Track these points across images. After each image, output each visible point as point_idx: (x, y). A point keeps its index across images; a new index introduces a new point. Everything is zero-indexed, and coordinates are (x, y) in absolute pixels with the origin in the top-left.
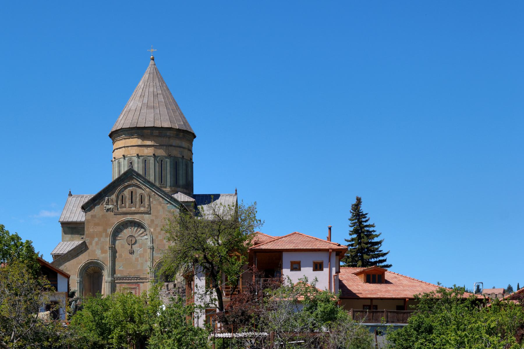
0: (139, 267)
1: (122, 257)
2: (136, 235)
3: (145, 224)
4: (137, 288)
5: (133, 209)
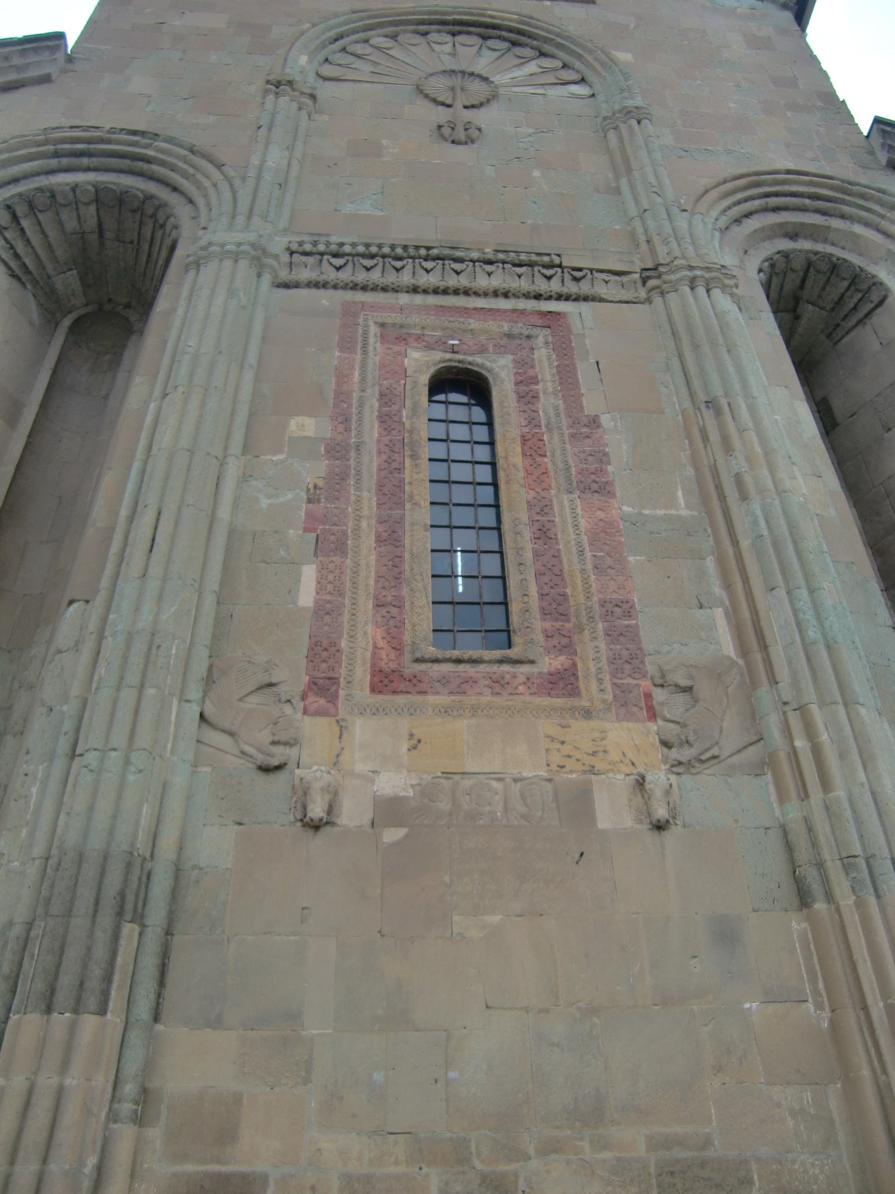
4: (529, 337)
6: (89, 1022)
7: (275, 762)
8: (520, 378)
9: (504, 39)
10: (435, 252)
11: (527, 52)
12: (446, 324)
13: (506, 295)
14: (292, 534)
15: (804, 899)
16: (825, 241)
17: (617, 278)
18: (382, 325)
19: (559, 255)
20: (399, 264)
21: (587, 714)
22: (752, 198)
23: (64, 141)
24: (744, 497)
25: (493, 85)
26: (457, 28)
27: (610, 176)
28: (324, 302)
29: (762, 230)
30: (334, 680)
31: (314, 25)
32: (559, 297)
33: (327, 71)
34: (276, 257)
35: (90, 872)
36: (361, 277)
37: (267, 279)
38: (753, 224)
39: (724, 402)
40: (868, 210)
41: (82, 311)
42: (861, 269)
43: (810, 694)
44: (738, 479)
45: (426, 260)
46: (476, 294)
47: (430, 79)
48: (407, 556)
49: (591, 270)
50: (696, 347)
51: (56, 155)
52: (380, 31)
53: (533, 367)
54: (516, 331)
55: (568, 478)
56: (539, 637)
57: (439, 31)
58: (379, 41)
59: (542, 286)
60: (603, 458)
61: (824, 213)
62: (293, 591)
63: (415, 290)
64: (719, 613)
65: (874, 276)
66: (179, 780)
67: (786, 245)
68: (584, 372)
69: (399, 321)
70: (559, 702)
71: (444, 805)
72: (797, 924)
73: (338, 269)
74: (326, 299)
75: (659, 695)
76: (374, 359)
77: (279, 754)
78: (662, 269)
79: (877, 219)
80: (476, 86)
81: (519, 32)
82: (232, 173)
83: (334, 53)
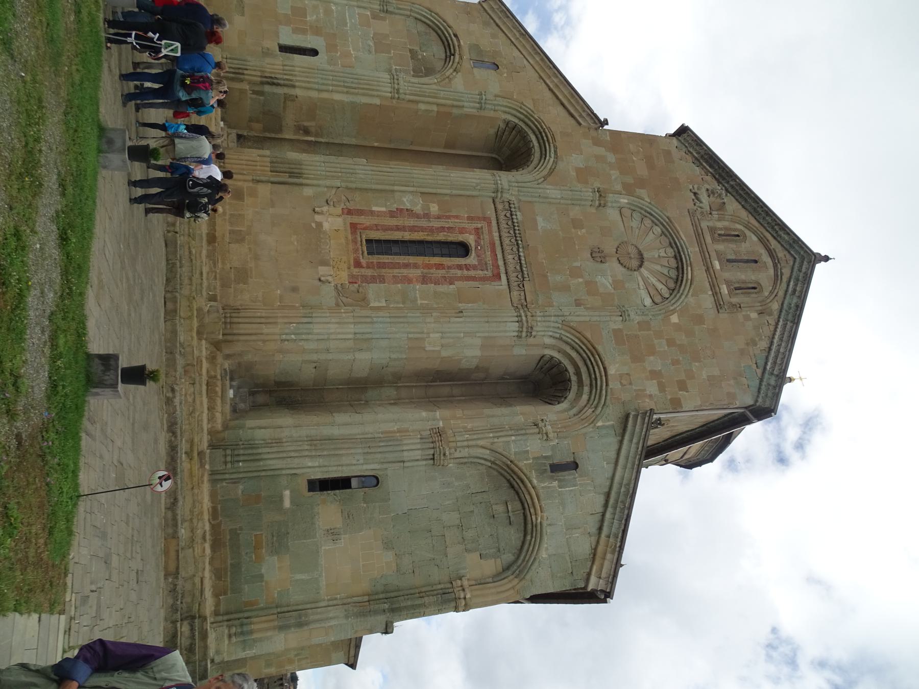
0: (555, 279)
1: (575, 227)
2: (642, 270)
3: (686, 296)
4: (487, 269)
8: (468, 266)
9: (678, 276)
10: (520, 242)
12: (486, 245)
13: (505, 264)
16: (579, 386)
17: (523, 298)
18: (482, 228)
20: (512, 232)
21: (349, 268)
22: (587, 354)
23: (546, 133)
26: (679, 258)
28: (489, 213)
29: (573, 359)
31: (650, 203)
33: (627, 212)
34: (502, 196)
35: (298, 166)
37: (493, 195)
38: (574, 354)
39: (460, 315)
40: (594, 400)
41: (500, 159)
42: (566, 398)
45: (516, 240)
46: (503, 255)
51: (540, 133)
53: (474, 270)
54: (488, 265)
55: (426, 274)
56: (371, 261)
58: (657, 230)
60: (437, 283)
61: (591, 385)
62: (377, 205)
63: (500, 237)
64: (385, 305)
65: (563, 402)
66: (321, 182)
67: (571, 370)
68: (476, 284)
69: (484, 232)
70: (352, 262)
71: (322, 236)
73: (505, 215)
74: (491, 213)
75: (356, 285)
76: (466, 226)
78: (525, 309)
79: (591, 402)
80: (635, 263)
81: (682, 281)
82: (540, 181)
83: (641, 213)
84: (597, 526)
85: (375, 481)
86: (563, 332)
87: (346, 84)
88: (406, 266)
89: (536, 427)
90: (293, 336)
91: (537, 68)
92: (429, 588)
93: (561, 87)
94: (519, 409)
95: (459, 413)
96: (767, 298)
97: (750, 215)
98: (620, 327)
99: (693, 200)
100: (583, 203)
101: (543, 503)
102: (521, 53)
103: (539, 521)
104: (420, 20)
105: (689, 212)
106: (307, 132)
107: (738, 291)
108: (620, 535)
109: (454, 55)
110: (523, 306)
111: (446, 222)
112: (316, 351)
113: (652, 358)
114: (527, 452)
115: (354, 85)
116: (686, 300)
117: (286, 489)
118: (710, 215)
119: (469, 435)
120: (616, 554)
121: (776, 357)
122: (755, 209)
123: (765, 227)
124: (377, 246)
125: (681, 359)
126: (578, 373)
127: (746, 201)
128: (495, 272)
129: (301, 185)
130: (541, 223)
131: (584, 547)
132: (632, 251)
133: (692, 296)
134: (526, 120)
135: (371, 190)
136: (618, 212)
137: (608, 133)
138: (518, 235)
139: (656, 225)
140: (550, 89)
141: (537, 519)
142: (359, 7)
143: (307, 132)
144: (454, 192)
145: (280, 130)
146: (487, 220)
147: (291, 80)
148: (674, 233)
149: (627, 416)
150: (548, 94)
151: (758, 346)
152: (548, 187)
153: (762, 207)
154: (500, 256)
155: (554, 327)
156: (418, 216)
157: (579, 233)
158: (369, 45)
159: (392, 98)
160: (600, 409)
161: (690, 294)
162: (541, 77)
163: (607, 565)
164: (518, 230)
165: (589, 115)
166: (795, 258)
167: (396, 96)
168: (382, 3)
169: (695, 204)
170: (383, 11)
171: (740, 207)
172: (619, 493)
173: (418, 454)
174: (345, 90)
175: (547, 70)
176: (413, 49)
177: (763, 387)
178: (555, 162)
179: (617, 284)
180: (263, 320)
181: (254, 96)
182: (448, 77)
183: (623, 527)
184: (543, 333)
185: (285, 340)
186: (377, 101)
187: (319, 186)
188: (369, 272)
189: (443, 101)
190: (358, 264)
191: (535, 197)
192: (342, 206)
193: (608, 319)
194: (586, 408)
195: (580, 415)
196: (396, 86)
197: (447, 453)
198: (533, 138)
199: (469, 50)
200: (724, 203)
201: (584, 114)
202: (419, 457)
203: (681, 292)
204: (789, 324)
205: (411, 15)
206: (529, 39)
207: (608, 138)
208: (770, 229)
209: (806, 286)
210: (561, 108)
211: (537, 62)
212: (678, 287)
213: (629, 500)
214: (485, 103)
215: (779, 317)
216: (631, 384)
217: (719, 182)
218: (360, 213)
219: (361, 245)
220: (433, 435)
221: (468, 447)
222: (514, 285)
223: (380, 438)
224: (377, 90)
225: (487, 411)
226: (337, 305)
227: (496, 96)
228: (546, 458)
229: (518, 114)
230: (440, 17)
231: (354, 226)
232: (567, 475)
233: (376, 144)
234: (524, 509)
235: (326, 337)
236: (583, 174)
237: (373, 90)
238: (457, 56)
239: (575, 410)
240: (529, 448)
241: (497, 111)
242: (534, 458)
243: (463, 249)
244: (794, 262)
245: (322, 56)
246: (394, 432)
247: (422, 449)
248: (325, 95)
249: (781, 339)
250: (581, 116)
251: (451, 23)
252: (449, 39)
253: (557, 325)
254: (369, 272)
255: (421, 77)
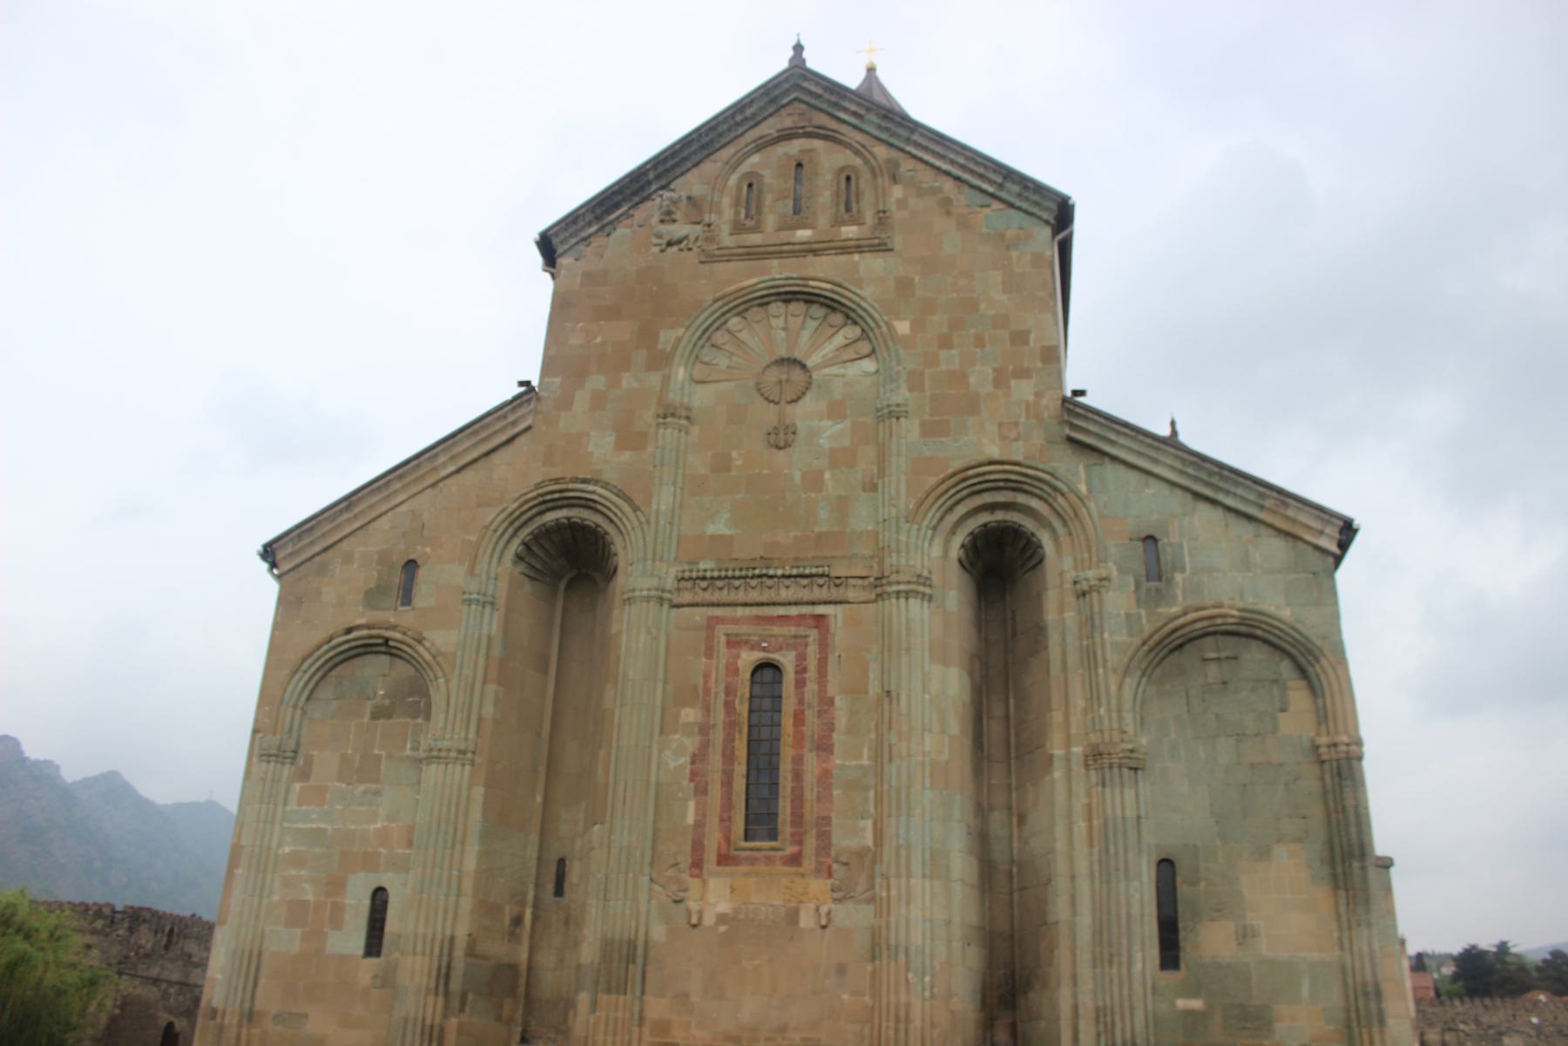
0: (824, 519)
1: (728, 469)
2: (810, 363)
4: (806, 637)
5: (804, 234)
6: (622, 998)
7: (678, 898)
8: (799, 668)
9: (822, 305)
10: (757, 572)
11: (838, 318)
13: (796, 604)
14: (685, 783)
15: (873, 958)
17: (860, 582)
18: (727, 635)
19: (829, 566)
20: (737, 583)
21: (803, 876)
24: (890, 760)
25: (808, 374)
27: (875, 471)
28: (698, 618)
30: (701, 861)
31: (688, 328)
32: (826, 603)
34: (670, 592)
36: (716, 596)
37: (666, 606)
38: (961, 510)
39: (894, 695)
41: (569, 576)
42: (1033, 534)
43: (893, 871)
44: (890, 746)
47: (767, 373)
48: (734, 794)
49: (847, 578)
50: (890, 650)
51: (544, 502)
52: (735, 312)
53: (805, 659)
54: (799, 633)
56: (788, 836)
57: (776, 301)
58: (734, 322)
59: (818, 594)
60: (831, 727)
61: (1014, 490)
63: (745, 605)
64: (869, 824)
65: (1039, 541)
66: (643, 909)
67: (985, 518)
71: (742, 916)
72: (869, 968)
73: (705, 589)
74: (699, 615)
75: (835, 866)
76: (723, 661)
77: (681, 894)
78: (884, 581)
79: (1045, 496)
80: (797, 374)
82: (643, 519)
83: (702, 347)
84: (1243, 522)
85: (1166, 867)
86: (926, 523)
87: (449, 844)
88: (798, 776)
89: (1087, 596)
90: (927, 979)
91: (415, 489)
92: (1330, 797)
93: (455, 451)
94: (1051, 615)
95: (1057, 716)
96: (866, 162)
97: (713, 157)
98: (916, 422)
99: (681, 250)
100: (682, 448)
101: (1208, 602)
102: (385, 513)
103: (1236, 613)
104: (312, 692)
105: (703, 262)
106: (518, 921)
107: (854, 207)
108: (1261, 489)
109: (387, 640)
110: (879, 586)
111: (716, 697)
112: (949, 942)
113: (972, 380)
114: (1128, 615)
115: (451, 831)
116: (870, 300)
117: (1173, 1004)
118: (712, 227)
119: (1099, 706)
120: (1289, 501)
121: (972, 172)
122: (703, 147)
123: (737, 137)
124: (761, 821)
125: (973, 331)
126: (992, 507)
127: (685, 159)
128: (811, 622)
129: (646, 943)
130: (718, 527)
131: (1275, 548)
132: (773, 375)
133: (861, 288)
134: (517, 524)
135: (655, 822)
136: (699, 388)
137: (547, 380)
138: (744, 573)
139: (725, 322)
140: (458, 471)
141: (1232, 616)
142: (285, 803)
143: (518, 921)
144: (661, 675)
145: (513, 968)
146: (712, 623)
147: (442, 942)
148: (743, 296)
149: (1071, 440)
150: (469, 476)
151: (952, 196)
152: (654, 507)
153: (700, 135)
154: (781, 611)
155: (917, 538)
156: (705, 745)
157: (739, 463)
158: (365, 793)
159: (472, 763)
160: (1059, 484)
161: (858, 291)
162: (434, 485)
163: (1303, 518)
164: (734, 570)
165: (513, 410)
166: (796, 99)
167: (469, 755)
168: (280, 759)
169: (690, 249)
170: (294, 758)
171: (695, 171)
172: (1196, 479)
173: (1129, 794)
174: (458, 847)
175: (421, 472)
176: (372, 713)
177: (1025, 205)
178: (606, 486)
179: (836, 411)
180: (902, 1026)
181: (467, 1010)
182: (434, 657)
183: (1249, 483)
184: (926, 558)
185: (932, 993)
186: (479, 791)
187: (648, 914)
188: (811, 842)
189: (480, 672)
190: (795, 860)
191: (671, 531)
192: (685, 876)
193: (903, 441)
194: (1056, 505)
195: (1066, 517)
196: (453, 754)
197: (1130, 746)
198: (550, 517)
199: (375, 609)
200: (689, 198)
201: (511, 418)
202: (1133, 791)
203: (853, 306)
204: (916, 137)
205: (302, 708)
206: (359, 495)
207: (558, 380)
208: (740, 131)
209: (849, 95)
210: (495, 458)
211: (405, 487)
212: (843, 309)
213: (1208, 465)
214: (485, 595)
215: (902, 150)
216: (1016, 424)
217: (647, 198)
218: (698, 846)
219: (759, 850)
220: (1097, 766)
221: (1119, 710)
222: (835, 594)
223: (1100, 850)
224: (460, 789)
225: (1055, 668)
226: (871, 900)
227: (471, 572)
228: (1138, 585)
229: (506, 536)
230: (310, 655)
231: (724, 859)
232: (1167, 556)
233: (539, 799)
234: (1214, 633)
235: (928, 925)
236: (629, 439)
237: (459, 797)
238: (388, 634)
239: (1057, 524)
240: (1122, 612)
241: (497, 575)
242: (1139, 603)
243: (767, 670)
244: (802, 101)
245: (387, 880)
246: (1090, 828)
247: (1122, 785)
248: (468, 885)
249: (942, 157)
250: (514, 424)
251: (318, 636)
252: (353, 644)
253: (914, 532)
254: (811, 842)
255: (429, 705)
